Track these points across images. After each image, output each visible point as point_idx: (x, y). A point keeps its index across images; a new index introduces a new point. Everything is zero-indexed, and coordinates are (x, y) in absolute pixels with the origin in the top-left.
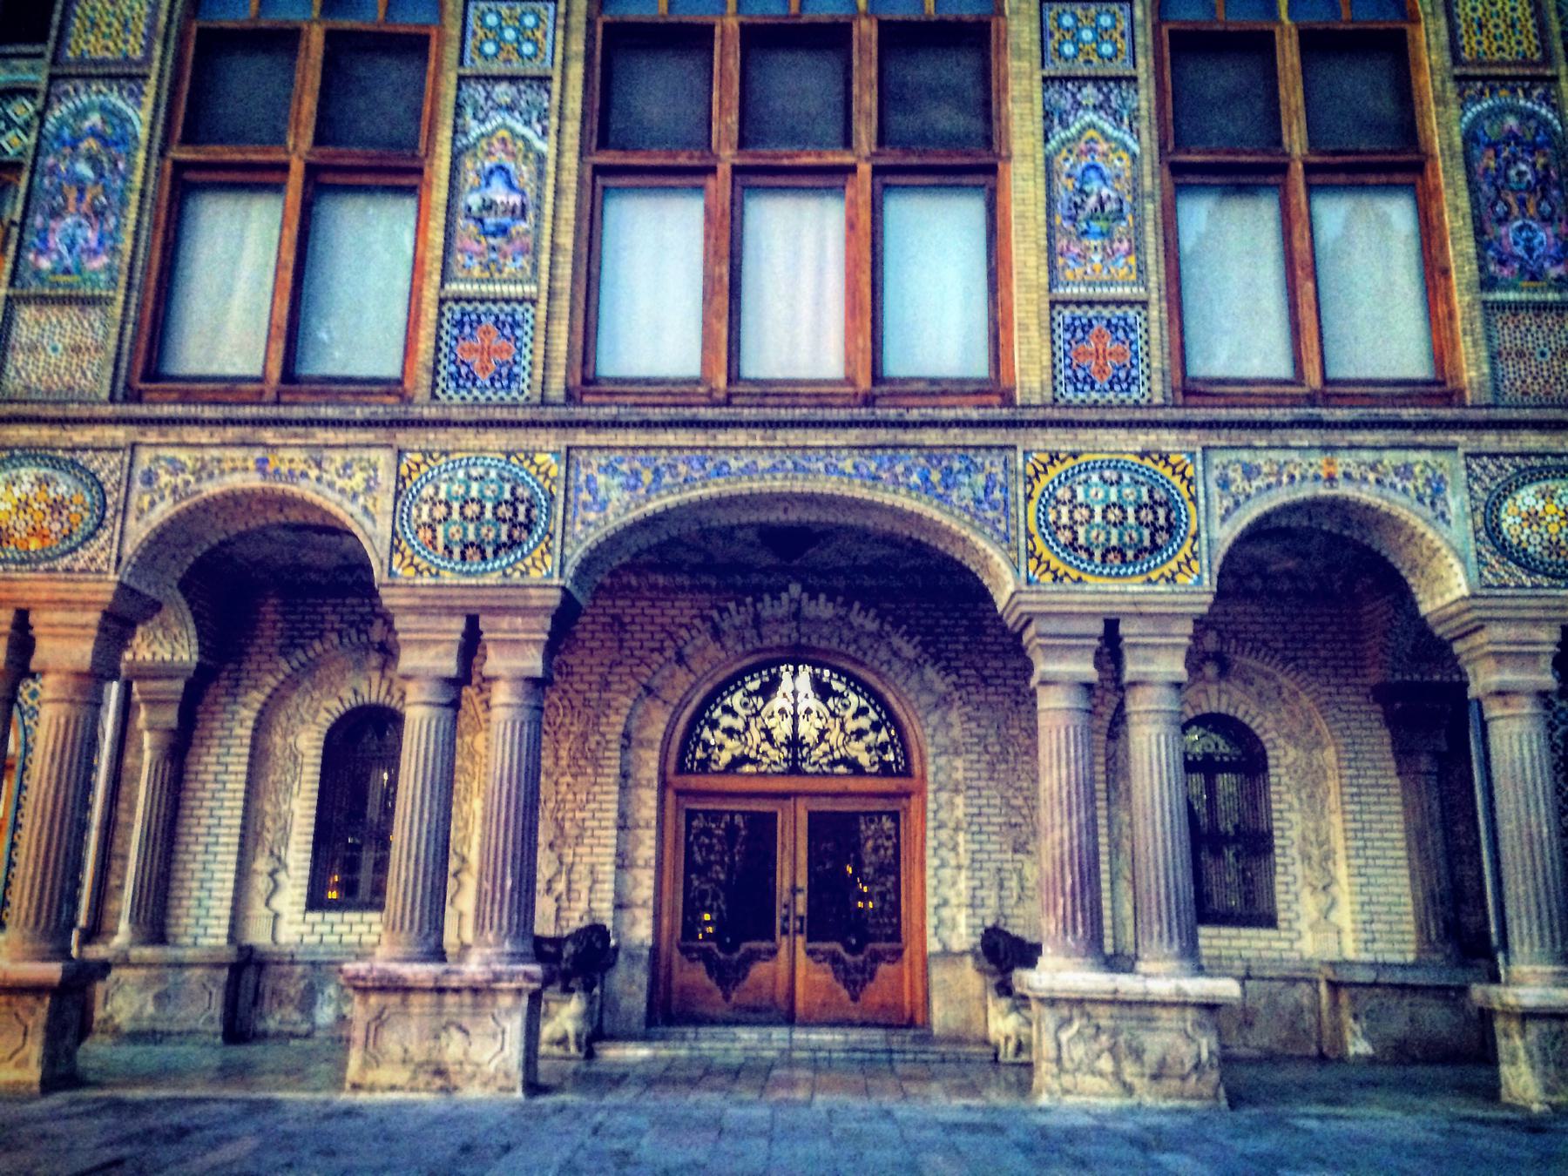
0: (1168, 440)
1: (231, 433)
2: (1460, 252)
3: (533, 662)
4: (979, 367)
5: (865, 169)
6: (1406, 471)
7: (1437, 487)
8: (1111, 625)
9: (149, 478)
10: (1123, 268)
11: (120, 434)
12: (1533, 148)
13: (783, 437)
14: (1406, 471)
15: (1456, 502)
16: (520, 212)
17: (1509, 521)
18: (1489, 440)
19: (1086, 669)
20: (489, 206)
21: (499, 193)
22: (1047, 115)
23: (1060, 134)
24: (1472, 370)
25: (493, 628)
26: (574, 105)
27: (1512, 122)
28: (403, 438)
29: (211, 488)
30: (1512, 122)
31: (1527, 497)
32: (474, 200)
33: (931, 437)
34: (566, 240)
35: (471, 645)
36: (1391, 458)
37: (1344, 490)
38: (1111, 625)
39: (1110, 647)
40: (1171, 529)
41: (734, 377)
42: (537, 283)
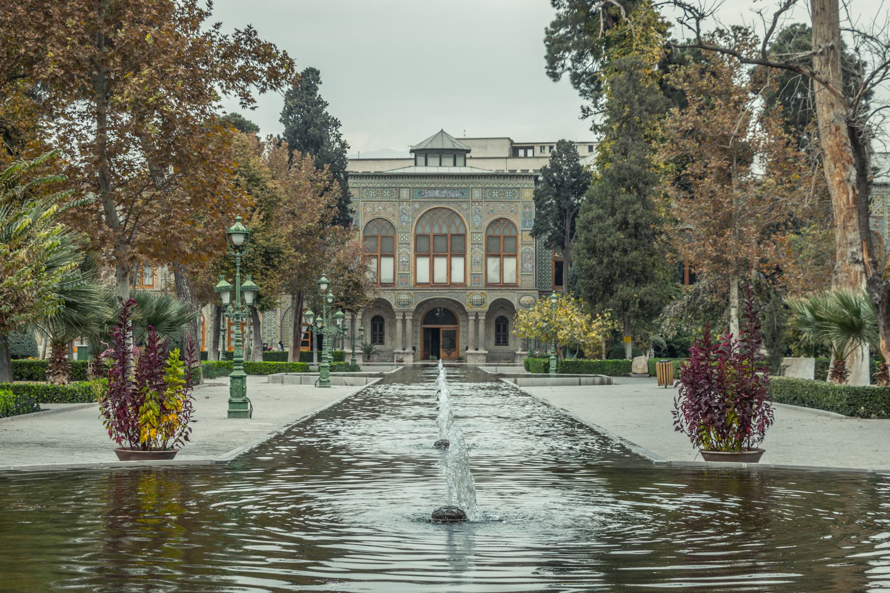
0: (484, 291)
2: (520, 267)
3: (411, 318)
4: (463, 281)
7: (513, 298)
8: (477, 313)
10: (480, 269)
15: (516, 299)
17: (521, 301)
18: (520, 292)
19: (474, 318)
21: (404, 259)
24: (520, 283)
25: (406, 314)
26: (413, 247)
31: (523, 299)
35: (404, 316)
38: (477, 313)
39: (477, 315)
41: (433, 283)
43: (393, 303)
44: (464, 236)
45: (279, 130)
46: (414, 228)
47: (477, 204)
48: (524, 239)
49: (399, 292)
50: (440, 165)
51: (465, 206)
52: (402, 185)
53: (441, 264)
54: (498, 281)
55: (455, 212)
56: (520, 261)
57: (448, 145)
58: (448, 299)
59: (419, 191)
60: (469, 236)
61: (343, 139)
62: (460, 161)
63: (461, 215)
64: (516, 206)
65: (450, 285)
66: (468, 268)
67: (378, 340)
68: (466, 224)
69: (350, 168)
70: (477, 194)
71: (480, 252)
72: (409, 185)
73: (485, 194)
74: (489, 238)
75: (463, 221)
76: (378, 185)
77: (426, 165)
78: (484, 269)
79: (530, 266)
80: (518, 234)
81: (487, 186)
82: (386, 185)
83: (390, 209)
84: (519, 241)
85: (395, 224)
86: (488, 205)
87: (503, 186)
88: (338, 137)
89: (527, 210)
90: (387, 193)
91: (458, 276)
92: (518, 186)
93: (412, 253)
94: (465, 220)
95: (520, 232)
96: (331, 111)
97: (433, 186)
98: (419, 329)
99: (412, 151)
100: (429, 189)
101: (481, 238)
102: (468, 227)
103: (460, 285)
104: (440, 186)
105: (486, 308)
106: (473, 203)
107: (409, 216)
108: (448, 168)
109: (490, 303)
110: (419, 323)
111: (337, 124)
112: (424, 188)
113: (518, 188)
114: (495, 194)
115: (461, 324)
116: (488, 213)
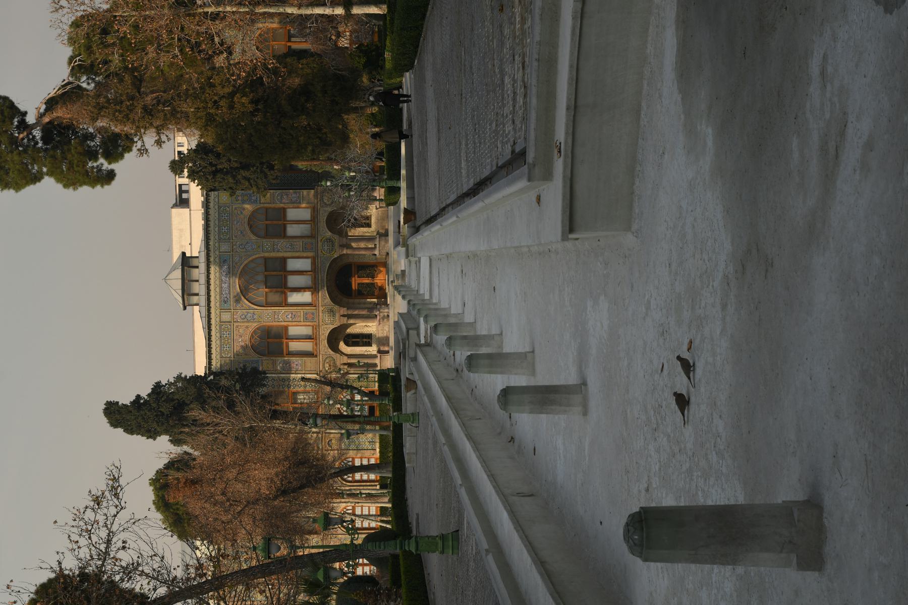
0: (319, 239)
1: (320, 344)
5: (285, 273)
6: (322, 214)
9: (326, 352)
11: (321, 356)
12: (282, 195)
13: (320, 282)
14: (322, 214)
16: (292, 314)
20: (291, 317)
21: (289, 316)
22: (278, 252)
23: (281, 250)
27: (279, 197)
28: (320, 324)
29: (327, 345)
30: (279, 197)
32: (291, 319)
33: (319, 266)
34: (295, 308)
36: (321, 215)
37: (325, 220)
40: (330, 239)
42: (301, 311)
43: (332, 327)
44: (266, 259)
45: (164, 440)
46: (259, 308)
47: (235, 247)
48: (268, 201)
49: (321, 321)
50: (197, 281)
51: (237, 259)
52: (218, 319)
53: (293, 281)
54: (309, 226)
55: (243, 268)
56: (291, 205)
57: (178, 273)
58: (327, 273)
59: (223, 303)
60: (266, 255)
61: (172, 380)
62: (195, 262)
63: (246, 262)
64: (236, 209)
65: (314, 270)
66: (297, 254)
67: (367, 340)
68: (254, 257)
69: (201, 371)
70: (225, 247)
71: (281, 243)
72: (218, 312)
73: (225, 239)
74: (267, 235)
75: (252, 261)
76: (218, 342)
77: (197, 295)
78: (297, 240)
79: (293, 195)
80: (264, 207)
81: (217, 237)
82: (218, 335)
83: (241, 331)
84: (270, 205)
85: (254, 325)
86: (236, 237)
87: (217, 222)
88: (170, 384)
89: (240, 198)
90: (226, 334)
91: (304, 264)
92: (216, 207)
93: (283, 310)
94: (250, 259)
95: (262, 205)
96: (145, 391)
97: (218, 290)
98: (357, 301)
99: (185, 308)
100: (221, 294)
101: (267, 243)
102: (257, 256)
103: (314, 263)
104: (217, 282)
105: (336, 237)
106: (235, 251)
107: (248, 313)
108: (199, 274)
109: (330, 233)
110: (351, 301)
111: (158, 386)
112: (220, 298)
113: (219, 207)
114: (225, 229)
115: (351, 260)
116: (244, 236)
